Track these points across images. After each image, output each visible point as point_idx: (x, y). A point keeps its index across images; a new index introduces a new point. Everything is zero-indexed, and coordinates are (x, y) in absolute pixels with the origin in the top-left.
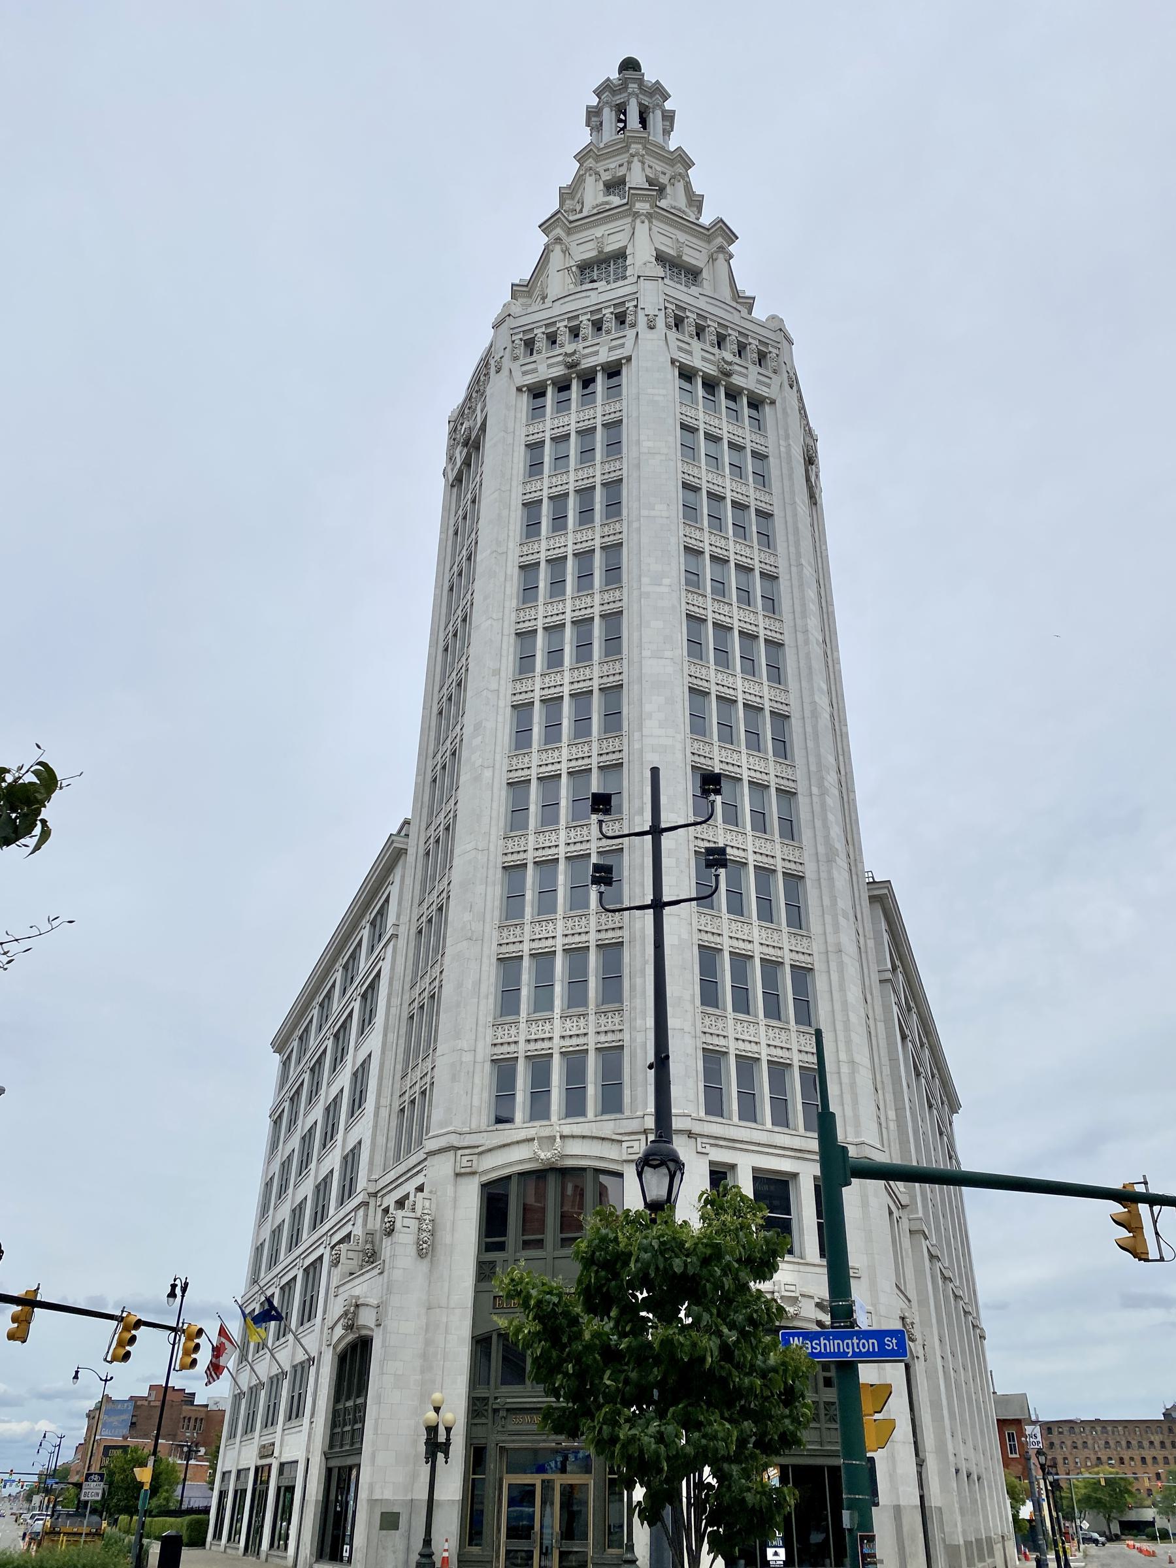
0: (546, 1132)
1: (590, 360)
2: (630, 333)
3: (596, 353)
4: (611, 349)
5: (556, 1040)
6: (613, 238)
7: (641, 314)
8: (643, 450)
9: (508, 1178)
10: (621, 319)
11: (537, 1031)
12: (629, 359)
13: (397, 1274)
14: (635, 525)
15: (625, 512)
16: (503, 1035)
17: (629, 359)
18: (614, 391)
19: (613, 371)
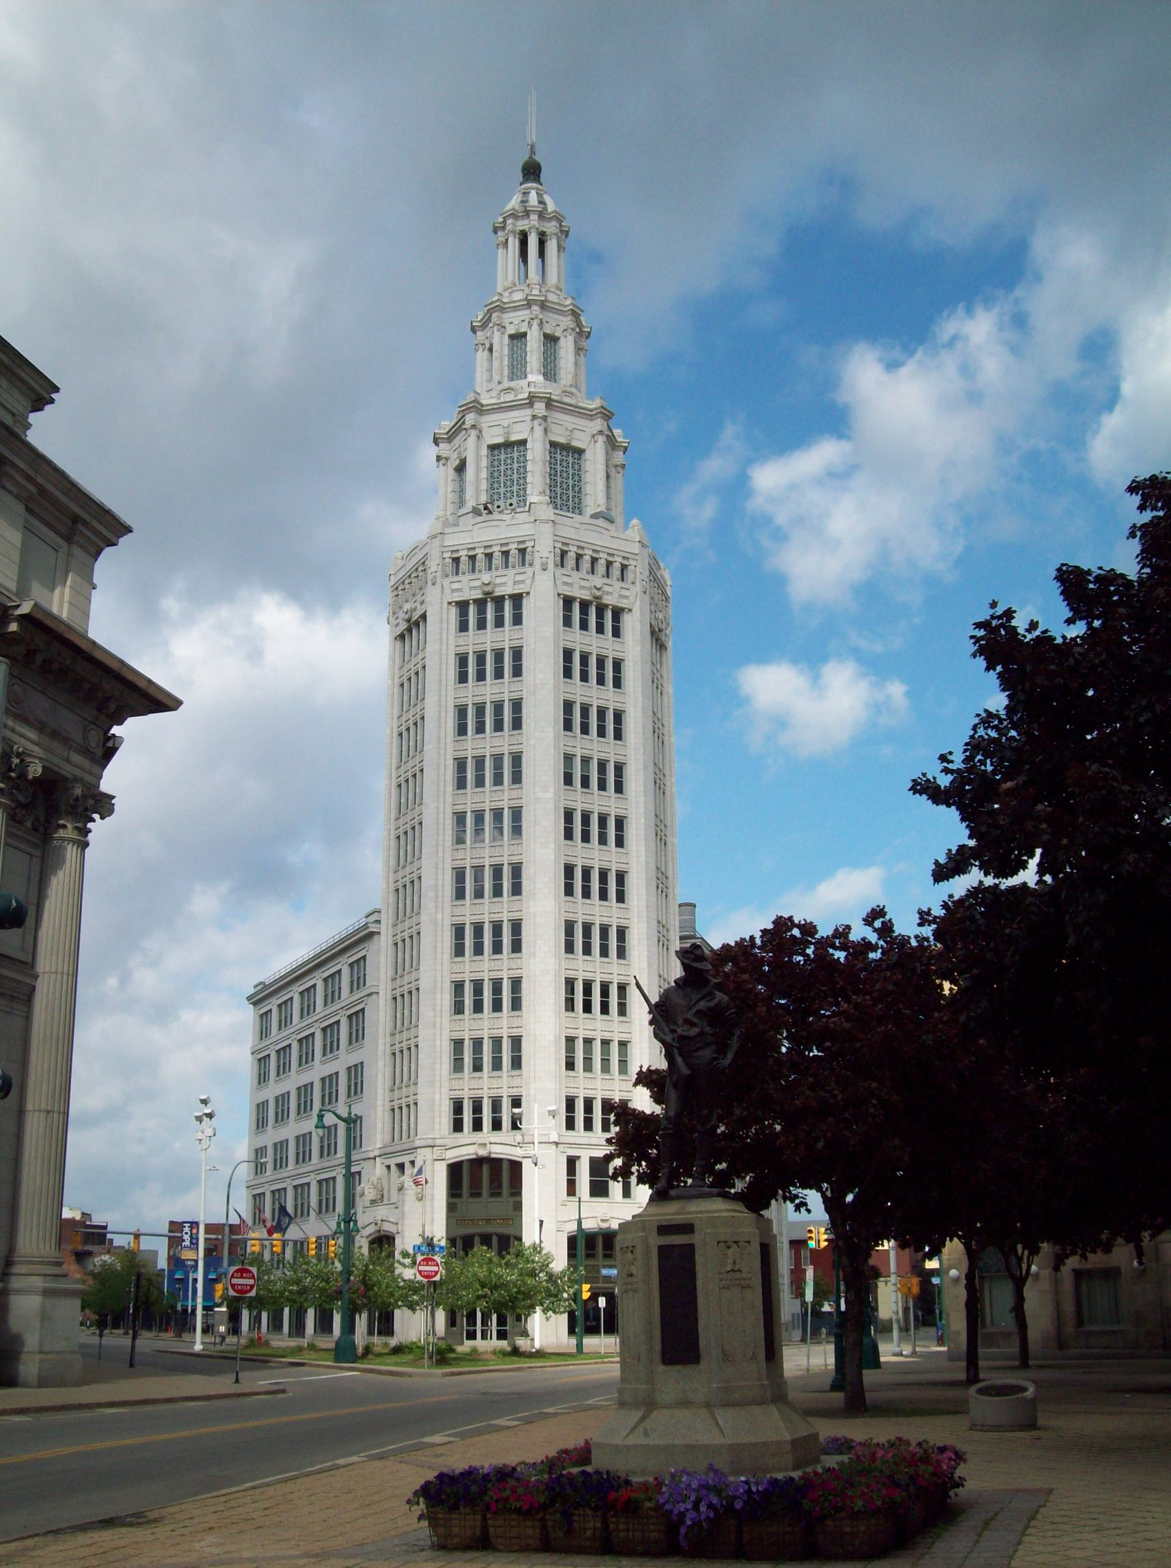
0: (480, 1141)
1: (503, 588)
2: (529, 571)
3: (504, 584)
4: (515, 583)
5: (486, 1089)
6: (517, 427)
7: (537, 555)
8: (538, 682)
9: (462, 1162)
10: (523, 551)
11: (474, 1084)
12: (528, 593)
13: (407, 1209)
14: (532, 742)
15: (524, 726)
16: (456, 968)
17: (528, 593)
18: (518, 620)
19: (517, 599)
